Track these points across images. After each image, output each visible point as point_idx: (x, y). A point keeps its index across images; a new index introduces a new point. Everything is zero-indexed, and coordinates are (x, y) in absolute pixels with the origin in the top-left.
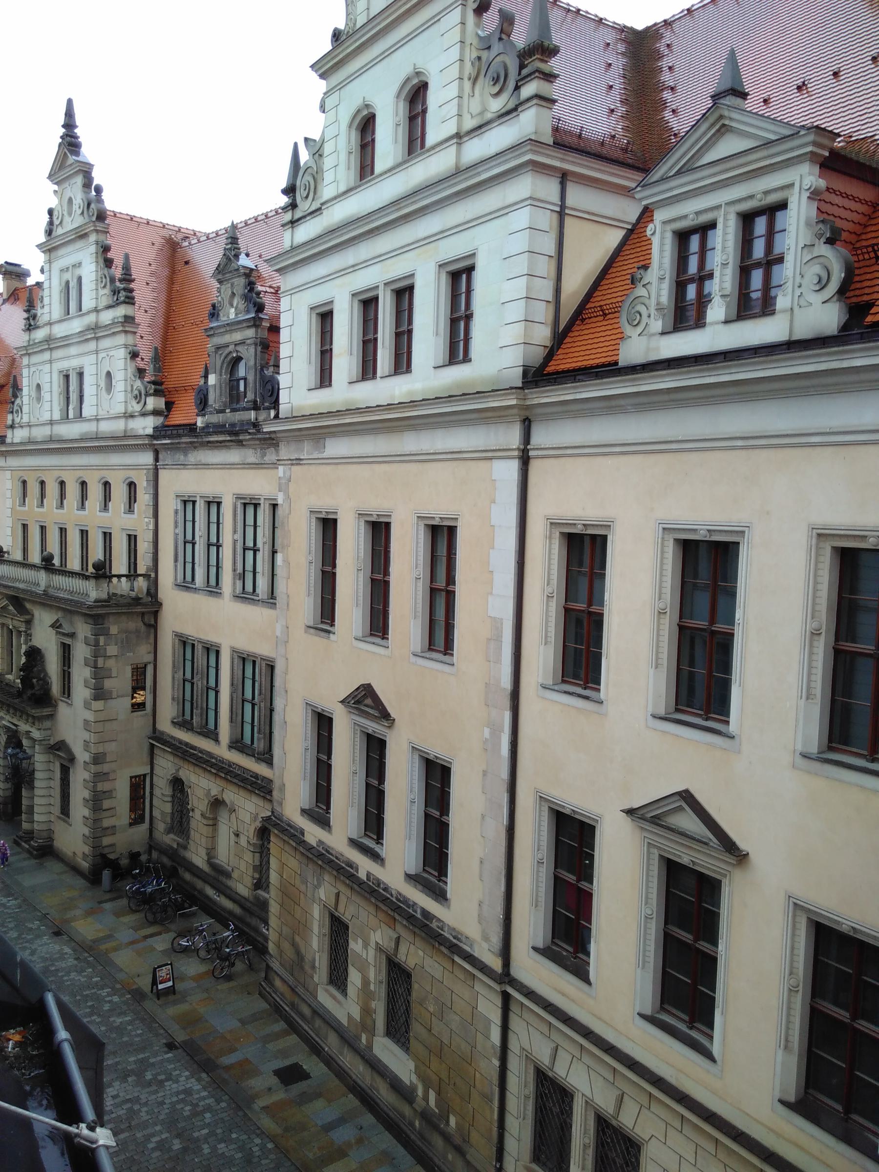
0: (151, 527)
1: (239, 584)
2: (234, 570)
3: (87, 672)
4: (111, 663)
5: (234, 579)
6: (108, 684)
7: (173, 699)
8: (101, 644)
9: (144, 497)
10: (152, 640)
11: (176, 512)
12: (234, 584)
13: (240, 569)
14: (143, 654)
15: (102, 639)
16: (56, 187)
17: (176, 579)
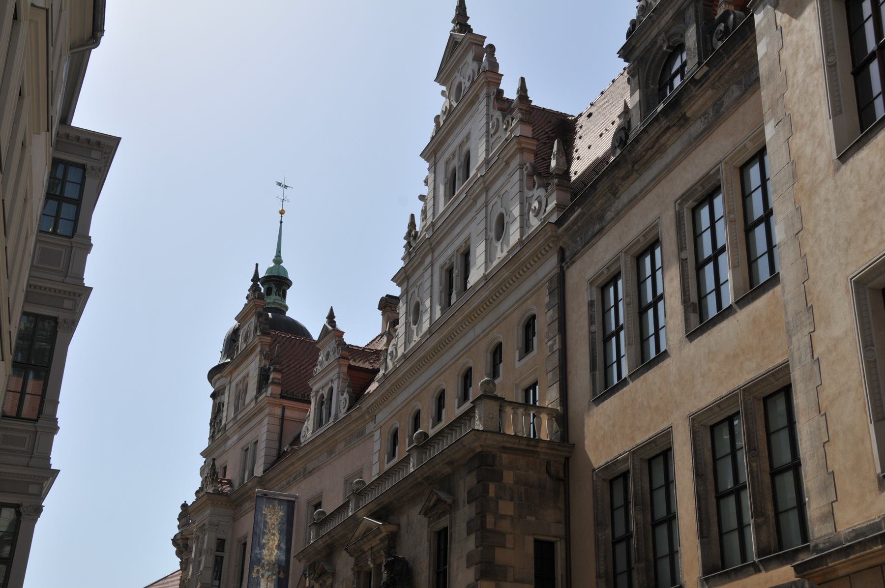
0: (557, 347)
1: (694, 318)
2: (685, 301)
3: (471, 544)
4: (505, 526)
5: (686, 313)
6: (502, 556)
7: (599, 576)
8: (492, 494)
9: (545, 321)
10: (561, 505)
11: (591, 304)
12: (687, 320)
13: (694, 298)
14: (549, 523)
15: (492, 487)
16: (444, 88)
17: (594, 393)
